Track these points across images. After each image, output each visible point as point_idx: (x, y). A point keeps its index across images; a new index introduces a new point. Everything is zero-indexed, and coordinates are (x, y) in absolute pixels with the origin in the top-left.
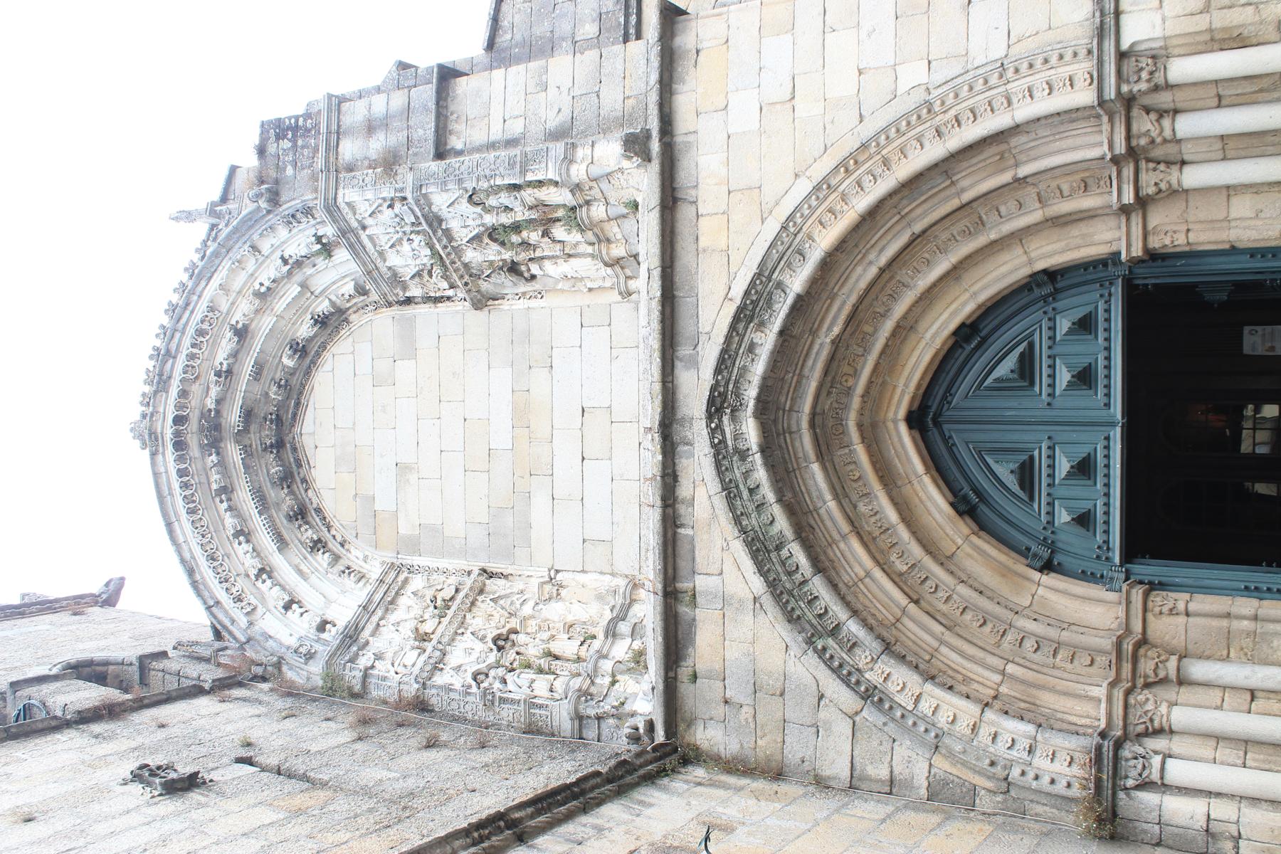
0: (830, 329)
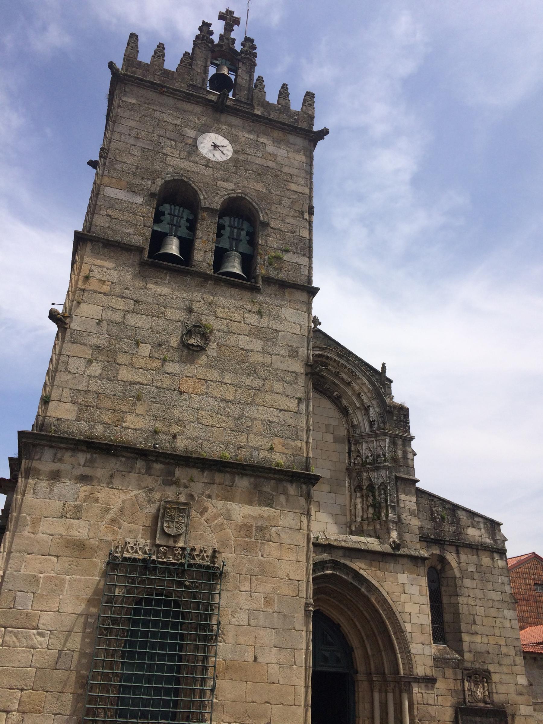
0: (350, 596)
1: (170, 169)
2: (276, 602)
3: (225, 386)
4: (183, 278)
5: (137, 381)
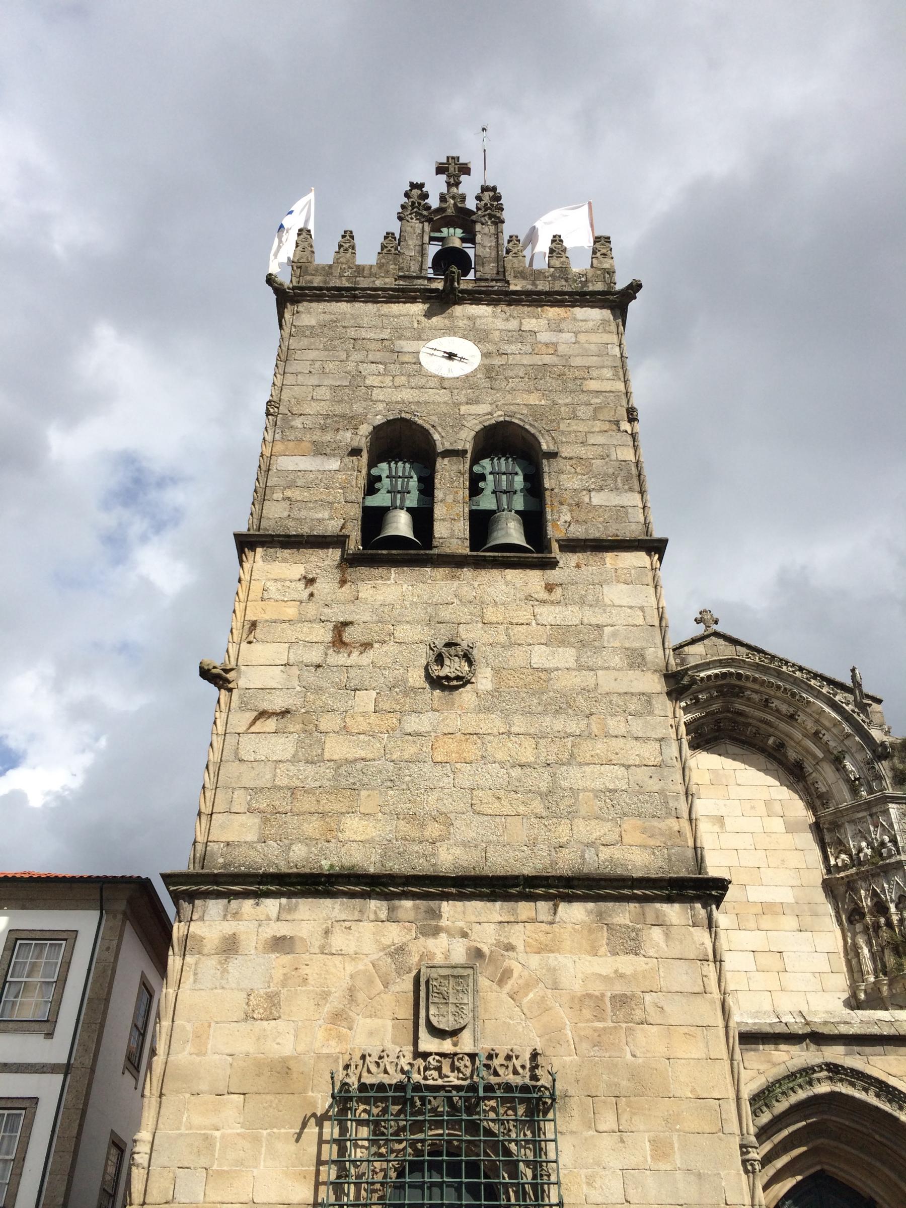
1: (381, 407)
2: (676, 1149)
3: (514, 739)
4: (419, 571)
5: (357, 756)
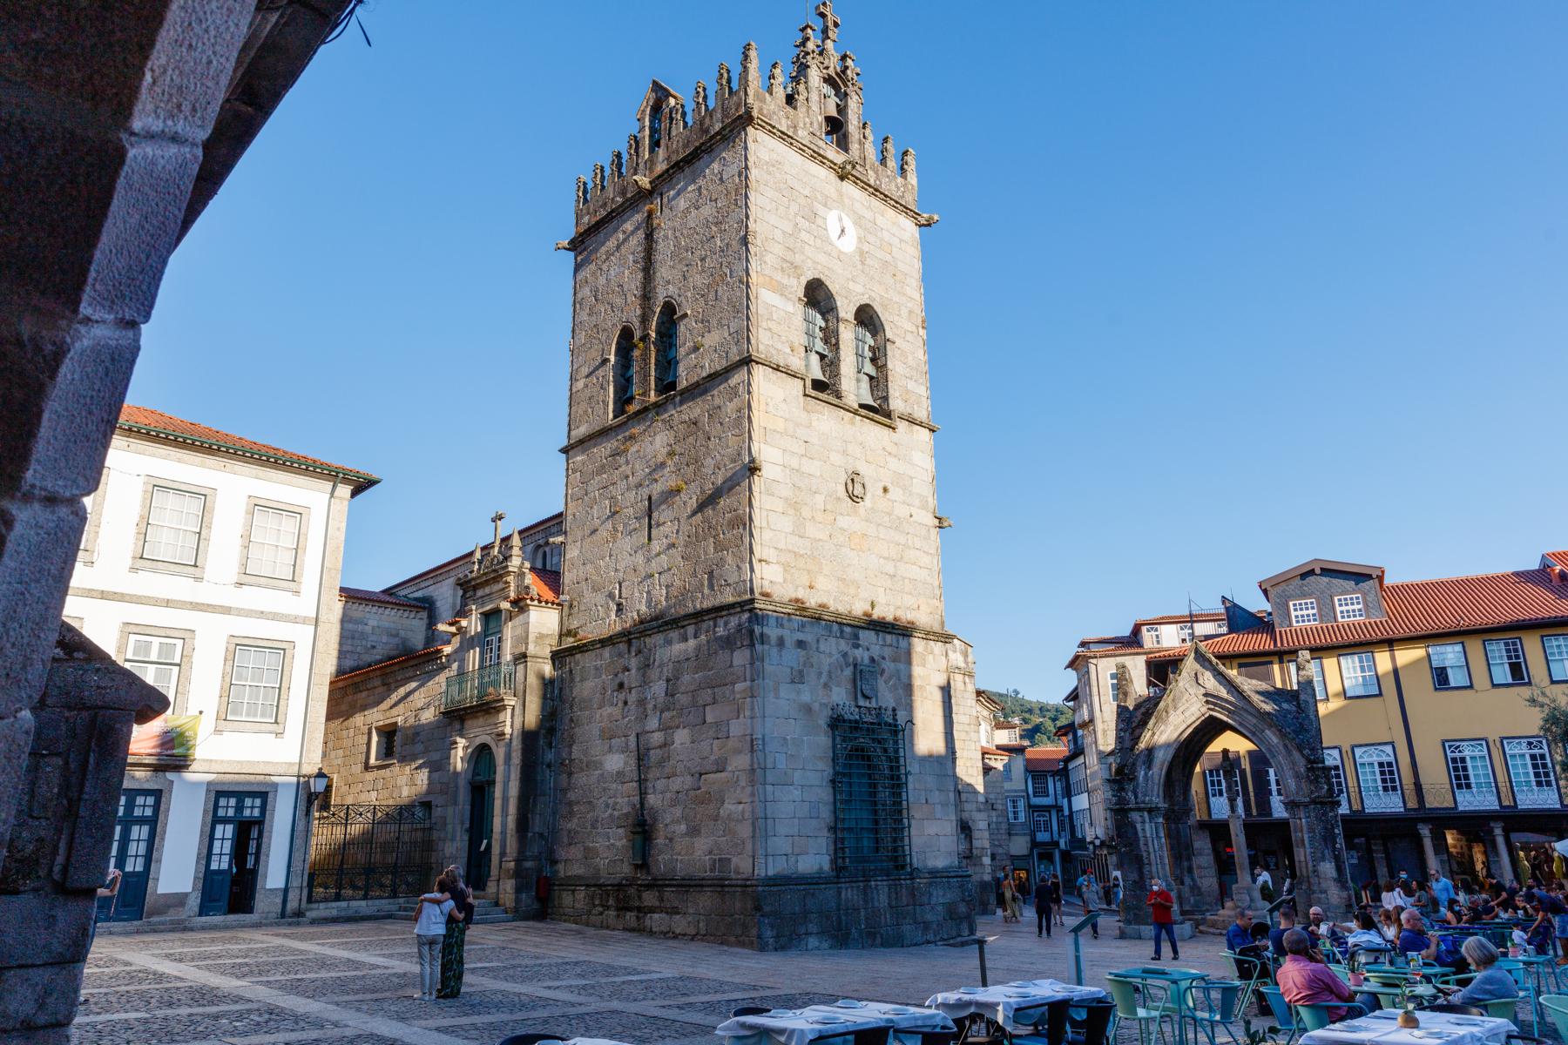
1: (810, 263)
